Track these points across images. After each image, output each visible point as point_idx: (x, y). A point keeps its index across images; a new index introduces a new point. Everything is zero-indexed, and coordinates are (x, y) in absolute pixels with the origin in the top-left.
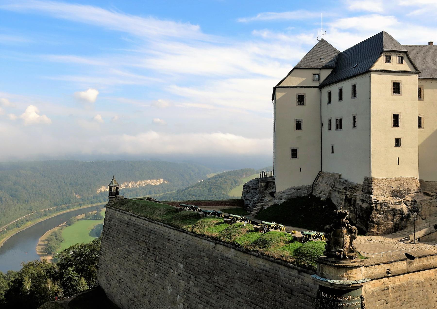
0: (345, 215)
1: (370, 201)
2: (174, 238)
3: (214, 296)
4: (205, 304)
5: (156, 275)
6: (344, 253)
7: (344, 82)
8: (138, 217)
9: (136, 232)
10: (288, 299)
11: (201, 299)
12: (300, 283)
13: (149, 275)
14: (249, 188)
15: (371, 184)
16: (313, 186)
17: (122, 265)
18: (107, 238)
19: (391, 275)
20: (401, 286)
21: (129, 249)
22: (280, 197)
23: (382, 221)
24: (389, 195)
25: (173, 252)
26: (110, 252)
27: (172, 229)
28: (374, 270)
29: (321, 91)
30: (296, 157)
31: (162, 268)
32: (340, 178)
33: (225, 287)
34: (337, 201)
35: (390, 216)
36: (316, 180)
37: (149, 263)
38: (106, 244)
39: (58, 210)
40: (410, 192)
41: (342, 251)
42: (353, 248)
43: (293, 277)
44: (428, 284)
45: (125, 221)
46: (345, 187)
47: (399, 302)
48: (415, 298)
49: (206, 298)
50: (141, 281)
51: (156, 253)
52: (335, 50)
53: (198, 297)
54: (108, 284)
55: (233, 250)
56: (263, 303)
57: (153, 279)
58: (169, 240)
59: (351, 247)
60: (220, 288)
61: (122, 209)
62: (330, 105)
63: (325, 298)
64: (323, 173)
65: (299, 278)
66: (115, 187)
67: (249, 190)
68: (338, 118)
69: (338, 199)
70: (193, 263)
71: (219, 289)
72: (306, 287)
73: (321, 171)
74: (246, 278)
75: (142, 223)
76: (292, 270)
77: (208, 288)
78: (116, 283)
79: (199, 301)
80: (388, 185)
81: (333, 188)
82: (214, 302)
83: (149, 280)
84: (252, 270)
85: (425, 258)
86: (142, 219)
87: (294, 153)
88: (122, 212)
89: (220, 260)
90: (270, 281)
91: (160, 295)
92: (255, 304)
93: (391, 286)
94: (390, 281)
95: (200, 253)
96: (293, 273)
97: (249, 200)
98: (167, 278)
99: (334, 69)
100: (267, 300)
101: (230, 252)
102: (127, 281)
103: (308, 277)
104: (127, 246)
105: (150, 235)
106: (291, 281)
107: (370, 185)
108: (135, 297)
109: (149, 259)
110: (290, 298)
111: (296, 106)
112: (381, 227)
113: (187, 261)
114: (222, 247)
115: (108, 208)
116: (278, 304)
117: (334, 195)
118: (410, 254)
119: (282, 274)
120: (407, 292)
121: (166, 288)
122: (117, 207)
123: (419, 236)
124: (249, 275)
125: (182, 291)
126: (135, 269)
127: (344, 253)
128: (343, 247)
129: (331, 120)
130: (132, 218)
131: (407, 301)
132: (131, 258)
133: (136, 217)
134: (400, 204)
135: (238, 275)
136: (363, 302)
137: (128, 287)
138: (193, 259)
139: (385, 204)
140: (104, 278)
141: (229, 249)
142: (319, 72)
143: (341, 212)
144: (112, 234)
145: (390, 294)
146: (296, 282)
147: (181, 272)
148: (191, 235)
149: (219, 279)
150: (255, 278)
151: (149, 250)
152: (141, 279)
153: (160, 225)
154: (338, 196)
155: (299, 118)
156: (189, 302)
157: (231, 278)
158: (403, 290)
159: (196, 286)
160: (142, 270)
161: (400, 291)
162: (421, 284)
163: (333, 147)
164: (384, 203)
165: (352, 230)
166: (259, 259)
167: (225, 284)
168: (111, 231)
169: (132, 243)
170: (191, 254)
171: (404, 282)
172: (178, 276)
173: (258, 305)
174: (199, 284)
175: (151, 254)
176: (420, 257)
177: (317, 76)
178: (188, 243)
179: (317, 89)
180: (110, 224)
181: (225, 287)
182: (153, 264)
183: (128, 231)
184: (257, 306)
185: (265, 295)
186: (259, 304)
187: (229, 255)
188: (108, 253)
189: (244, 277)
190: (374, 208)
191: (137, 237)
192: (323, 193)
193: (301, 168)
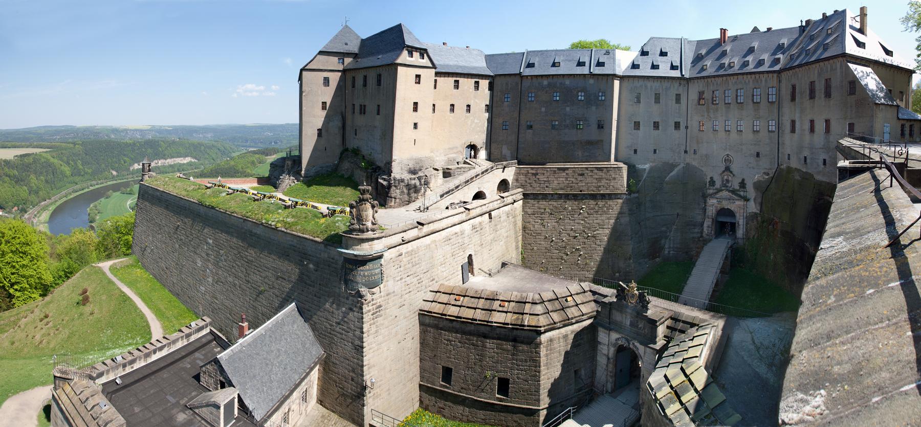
20: (412, 251)
23: (398, 196)
35: (405, 191)
85: (432, 224)
93: (404, 251)
112: (398, 200)
120: (416, 255)
161: (412, 255)
162: (428, 247)
171: (415, 247)
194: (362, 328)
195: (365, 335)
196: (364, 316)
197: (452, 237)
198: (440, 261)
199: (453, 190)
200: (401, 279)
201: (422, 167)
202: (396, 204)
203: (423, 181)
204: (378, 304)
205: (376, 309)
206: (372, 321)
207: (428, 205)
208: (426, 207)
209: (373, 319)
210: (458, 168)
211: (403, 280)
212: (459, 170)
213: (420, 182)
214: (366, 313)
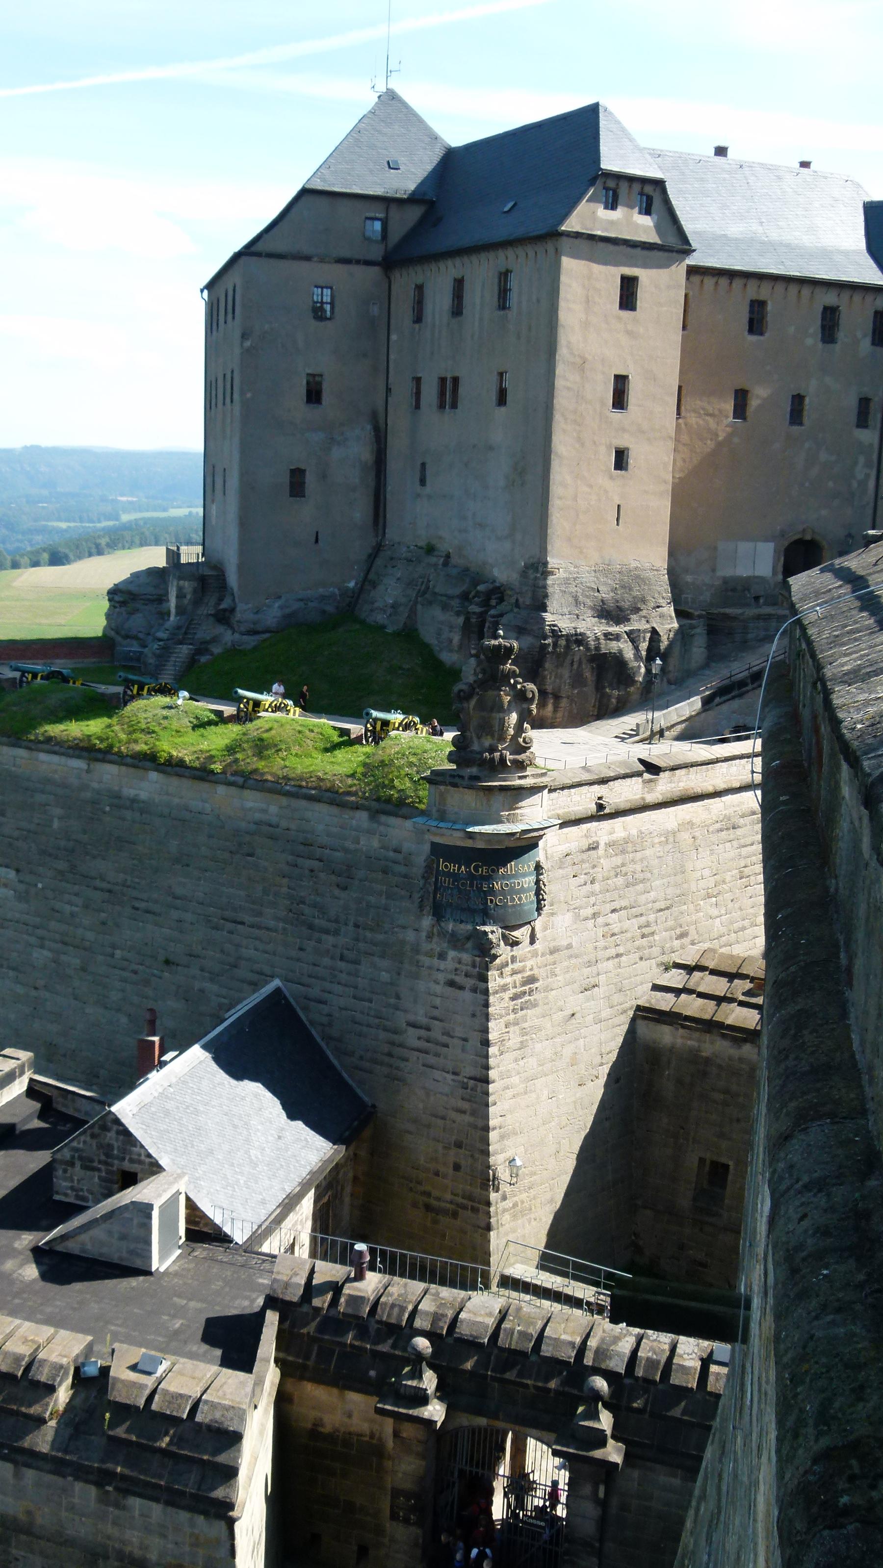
0: (510, 650)
1: (539, 629)
4: (59, 946)
6: (501, 755)
7: (474, 258)
10: (337, 892)
12: (375, 843)
14: (133, 599)
15: (545, 579)
19: (607, 811)
20: (626, 841)
22: (252, 626)
24: (590, 613)
28: (569, 799)
29: (389, 278)
33: (128, 887)
35: (588, 674)
40: (642, 607)
41: (497, 750)
42: (524, 741)
43: (354, 833)
44: (685, 836)
47: (620, 881)
48: (656, 871)
52: (436, 138)
56: (260, 914)
59: (521, 740)
60: (110, 891)
63: (449, 874)
65: (370, 832)
76: (351, 813)
80: (588, 585)
82: (90, 935)
85: (683, 772)
89: (108, 809)
92: (235, 922)
93: (603, 840)
94: (602, 826)
96: (354, 822)
97: (135, 638)
107: (541, 583)
112: (564, 703)
116: (307, 910)
118: (649, 761)
120: (639, 855)
123: (662, 723)
127: (501, 755)
128: (502, 739)
131: (636, 876)
134: (617, 637)
136: (541, 877)
139: (579, 639)
143: (500, 645)
145: (602, 861)
146: (362, 843)
158: (630, 849)
161: (623, 852)
162: (671, 836)
164: (576, 634)
165: (526, 690)
166: (247, 793)
167: (129, 878)
171: (634, 832)
173: (243, 923)
176: (673, 769)
177: (378, 225)
181: (128, 887)
186: (247, 919)
190: (550, 649)
193: (317, 533)
194: (486, 1031)
195: (492, 1050)
196: (492, 999)
197: (742, 821)
198: (702, 884)
199: (742, 684)
200: (595, 916)
201: (644, 601)
202: (559, 714)
203: (644, 646)
204: (528, 973)
205: (524, 984)
206: (512, 1017)
207: (664, 724)
208: (656, 728)
209: (514, 1011)
210: (759, 617)
211: (600, 920)
212: (762, 624)
213: (636, 648)
214: (496, 992)
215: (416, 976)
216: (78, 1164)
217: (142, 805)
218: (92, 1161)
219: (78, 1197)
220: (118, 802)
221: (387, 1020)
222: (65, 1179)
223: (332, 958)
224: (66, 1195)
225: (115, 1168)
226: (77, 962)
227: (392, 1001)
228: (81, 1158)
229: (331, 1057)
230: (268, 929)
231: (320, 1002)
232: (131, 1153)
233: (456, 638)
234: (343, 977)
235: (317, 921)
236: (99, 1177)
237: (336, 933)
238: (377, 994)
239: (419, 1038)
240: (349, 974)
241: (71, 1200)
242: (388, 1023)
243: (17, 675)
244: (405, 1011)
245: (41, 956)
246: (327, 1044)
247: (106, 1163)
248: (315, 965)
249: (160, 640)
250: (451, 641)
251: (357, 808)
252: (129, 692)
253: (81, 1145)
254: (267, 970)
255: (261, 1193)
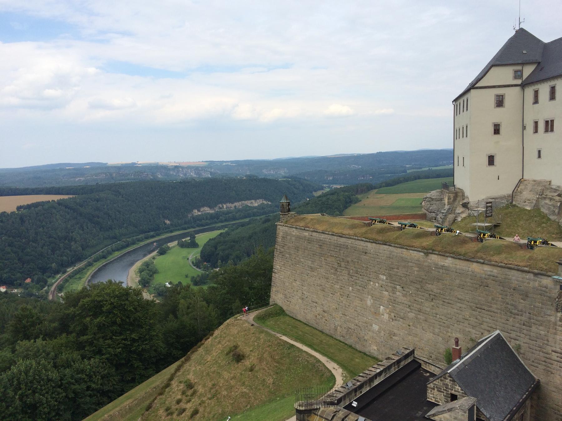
2: (372, 251)
3: (427, 304)
5: (351, 288)
8: (322, 233)
9: (320, 248)
10: (522, 301)
11: (411, 307)
13: (341, 289)
16: (513, 194)
17: (304, 281)
18: (281, 256)
21: (313, 265)
25: (372, 265)
26: (288, 270)
27: (369, 242)
30: (494, 165)
31: (358, 281)
32: (550, 184)
34: (549, 208)
36: (516, 188)
37: (341, 278)
38: (281, 261)
39: (147, 238)
45: (305, 237)
46: (559, 194)
49: (419, 306)
50: (332, 295)
51: (349, 267)
53: (408, 306)
54: (287, 301)
55: (450, 259)
56: (491, 307)
57: (348, 293)
58: (366, 253)
60: (435, 295)
61: (299, 226)
62: (537, 105)
64: (525, 180)
66: (288, 204)
67: (432, 202)
68: (548, 120)
69: (550, 207)
70: (399, 274)
71: (433, 297)
72: (544, 289)
73: (522, 178)
74: (469, 284)
75: (329, 238)
76: (526, 274)
77: (420, 296)
78: (297, 300)
79: (408, 310)
81: (542, 196)
82: (428, 310)
83: (342, 294)
84: (476, 276)
86: (328, 234)
87: (491, 160)
88: (301, 229)
89: (434, 268)
90: (499, 286)
91: (358, 308)
92: (481, 309)
95: (408, 264)
96: (527, 276)
97: (434, 212)
98: (365, 290)
99: (539, 63)
100: (496, 304)
101: (447, 261)
102: (313, 297)
103: (546, 279)
104: (311, 262)
105: (340, 250)
106: (525, 284)
108: (324, 311)
109: (341, 273)
110: (525, 300)
111: (495, 108)
113: (391, 272)
114: (436, 256)
115: (281, 225)
116: (509, 306)
117: (543, 203)
119: (514, 278)
121: (364, 300)
122: (292, 224)
124: (471, 281)
125: (386, 302)
126: (323, 284)
129: (537, 122)
130: (314, 234)
132: (316, 274)
133: (320, 232)
135: (458, 281)
137: (314, 302)
138: (398, 269)
140: (280, 296)
141: (444, 258)
142: (522, 68)
144: (287, 251)
147: (384, 283)
148: (395, 247)
149: (434, 288)
150: (480, 284)
151: (340, 265)
152: (331, 294)
153: (353, 239)
154: (550, 204)
155: (497, 121)
156: (396, 312)
157: (449, 286)
159: (404, 296)
160: (332, 284)
163: (539, 152)
166: (484, 266)
167: (442, 292)
168: (286, 248)
169: (315, 258)
170: (396, 265)
172: (381, 288)
173: (484, 310)
174: (408, 293)
175: (343, 269)
178: (390, 254)
179: (518, 88)
180: (284, 242)
182: (346, 278)
183: (309, 247)
184: (483, 310)
185: (493, 299)
186: (486, 308)
187: (446, 264)
188: (285, 271)
189: (465, 284)
191: (323, 252)
192: (527, 201)
215: (555, 334)
216: (436, 389)
217: (446, 268)
218: (441, 389)
219: (435, 401)
220: (437, 266)
221: (544, 349)
222: (431, 394)
223: (520, 324)
224: (431, 399)
225: (449, 393)
226: (423, 318)
227: (546, 342)
228: (437, 387)
229: (521, 360)
230: (494, 312)
231: (515, 340)
232: (455, 388)
233: (557, 211)
234: (525, 331)
235: (513, 311)
236: (443, 395)
237: (522, 315)
238: (539, 339)
239: (557, 357)
240: (527, 330)
241: (434, 401)
242: (544, 350)
243: (400, 225)
244: (551, 346)
245: (411, 315)
246: (519, 355)
247: (446, 390)
248: (513, 326)
249: (443, 213)
250: (555, 212)
251: (529, 272)
252: (438, 231)
253: (437, 383)
254: (494, 326)
255: (502, 409)
